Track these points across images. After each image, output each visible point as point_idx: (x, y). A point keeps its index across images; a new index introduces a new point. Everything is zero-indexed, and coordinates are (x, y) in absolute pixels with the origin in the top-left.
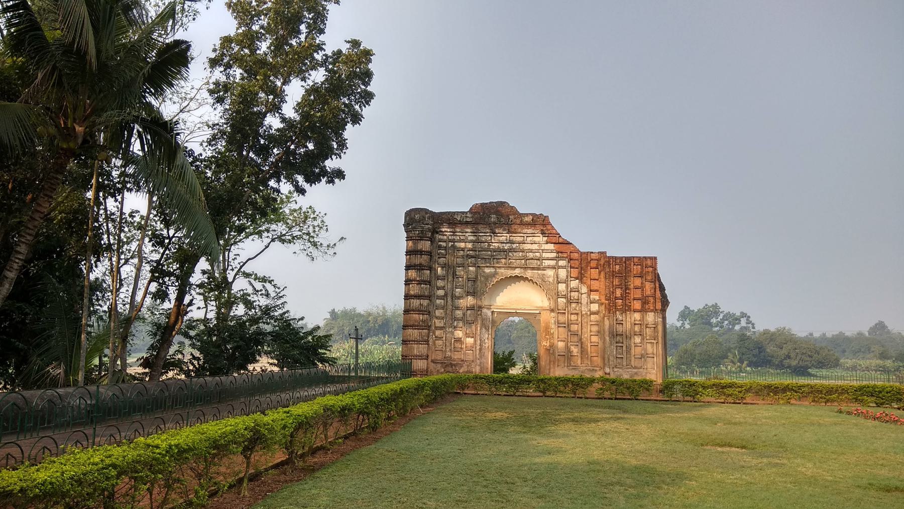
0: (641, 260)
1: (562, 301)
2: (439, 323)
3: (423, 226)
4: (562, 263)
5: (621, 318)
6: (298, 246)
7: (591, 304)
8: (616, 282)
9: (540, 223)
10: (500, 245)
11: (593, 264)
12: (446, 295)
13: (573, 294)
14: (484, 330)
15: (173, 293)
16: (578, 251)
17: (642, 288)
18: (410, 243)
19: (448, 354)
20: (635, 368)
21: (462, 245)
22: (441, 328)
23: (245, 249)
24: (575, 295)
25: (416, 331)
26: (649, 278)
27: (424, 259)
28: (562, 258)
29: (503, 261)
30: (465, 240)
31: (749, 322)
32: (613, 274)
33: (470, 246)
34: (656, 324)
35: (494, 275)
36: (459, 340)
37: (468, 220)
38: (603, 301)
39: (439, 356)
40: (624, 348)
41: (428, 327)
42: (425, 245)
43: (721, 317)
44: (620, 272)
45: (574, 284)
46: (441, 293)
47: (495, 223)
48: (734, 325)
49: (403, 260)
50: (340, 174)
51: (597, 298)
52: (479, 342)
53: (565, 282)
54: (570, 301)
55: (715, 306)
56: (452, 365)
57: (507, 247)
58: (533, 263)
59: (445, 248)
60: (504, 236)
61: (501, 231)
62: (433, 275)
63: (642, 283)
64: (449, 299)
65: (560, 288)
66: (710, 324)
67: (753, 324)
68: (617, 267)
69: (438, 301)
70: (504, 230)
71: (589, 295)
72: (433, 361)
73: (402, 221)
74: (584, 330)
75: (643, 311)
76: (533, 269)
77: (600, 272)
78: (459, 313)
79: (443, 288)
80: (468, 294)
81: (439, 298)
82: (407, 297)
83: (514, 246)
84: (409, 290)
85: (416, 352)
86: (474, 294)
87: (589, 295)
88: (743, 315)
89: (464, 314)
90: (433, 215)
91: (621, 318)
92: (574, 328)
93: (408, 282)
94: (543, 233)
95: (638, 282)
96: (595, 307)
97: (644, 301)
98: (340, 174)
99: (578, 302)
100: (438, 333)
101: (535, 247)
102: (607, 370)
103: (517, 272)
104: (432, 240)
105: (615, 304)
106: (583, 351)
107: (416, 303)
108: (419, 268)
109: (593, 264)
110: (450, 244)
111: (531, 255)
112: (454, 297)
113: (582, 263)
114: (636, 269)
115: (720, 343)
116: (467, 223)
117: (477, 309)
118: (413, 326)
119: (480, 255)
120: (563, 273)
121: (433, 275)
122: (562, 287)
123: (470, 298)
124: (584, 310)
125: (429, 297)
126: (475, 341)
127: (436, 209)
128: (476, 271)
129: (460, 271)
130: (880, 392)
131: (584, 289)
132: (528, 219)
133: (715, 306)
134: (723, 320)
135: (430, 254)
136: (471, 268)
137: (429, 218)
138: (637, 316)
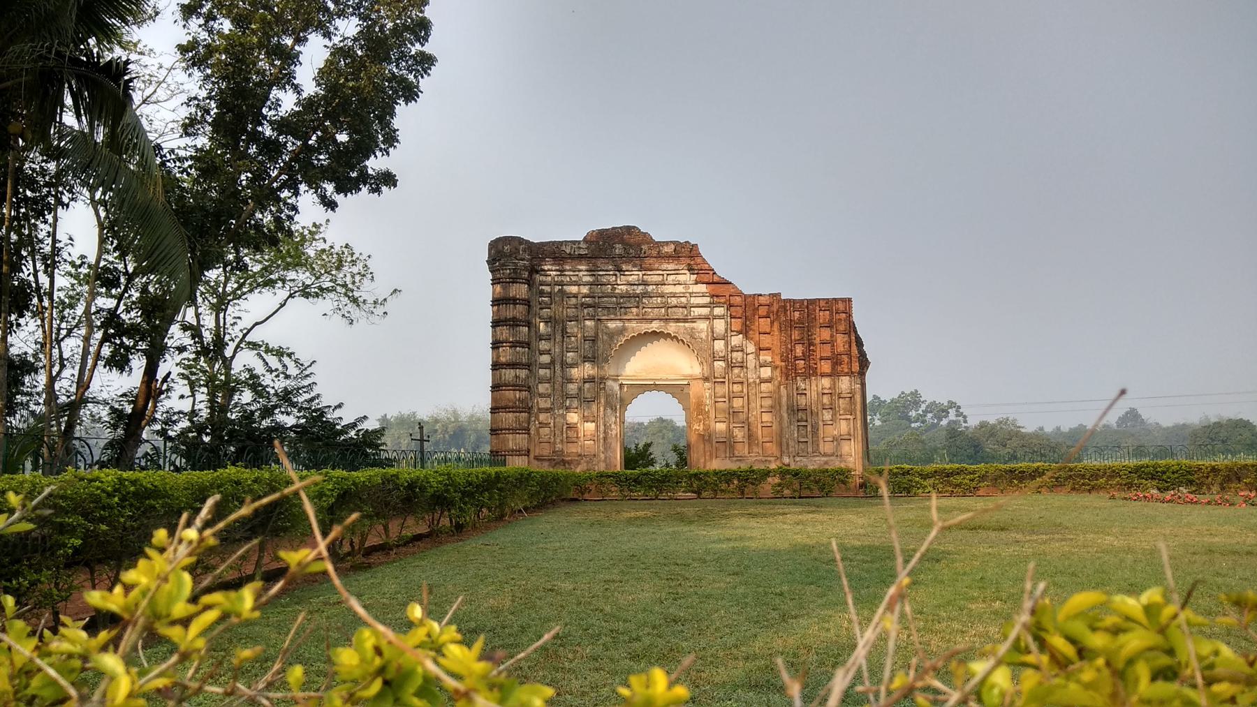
0: (830, 304)
1: (719, 365)
2: (544, 403)
3: (514, 262)
4: (718, 311)
5: (803, 386)
7: (761, 369)
8: (796, 335)
9: (686, 254)
10: (629, 288)
11: (763, 311)
12: (553, 362)
13: (735, 354)
14: (609, 410)
15: (138, 364)
16: (740, 294)
17: (832, 342)
18: (498, 288)
19: (559, 446)
20: (825, 455)
21: (574, 289)
22: (547, 410)
23: (253, 307)
24: (738, 356)
25: (511, 415)
26: (842, 328)
27: (518, 311)
28: (719, 305)
29: (634, 310)
31: (959, 414)
32: (791, 325)
33: (585, 290)
34: (852, 392)
35: (622, 331)
36: (571, 427)
37: (582, 252)
38: (778, 363)
39: (546, 451)
40: (809, 428)
41: (528, 410)
42: (520, 290)
43: (923, 407)
44: (800, 321)
45: (737, 340)
46: (545, 359)
47: (621, 257)
48: (940, 419)
49: (488, 313)
50: (388, 179)
51: (769, 359)
52: (602, 428)
54: (730, 366)
55: (915, 394)
56: (564, 462)
57: (639, 290)
59: (550, 295)
60: (635, 275)
61: (630, 268)
62: (533, 333)
63: (832, 336)
64: (558, 367)
65: (716, 347)
66: (909, 419)
67: (965, 417)
68: (797, 314)
69: (542, 372)
70: (635, 266)
71: (758, 356)
72: (536, 458)
73: (485, 256)
74: (752, 405)
75: (834, 374)
76: (678, 320)
77: (772, 323)
78: (572, 388)
79: (548, 352)
80: (586, 359)
81: (544, 366)
82: (496, 366)
83: (650, 288)
84: (498, 357)
85: (511, 445)
86: (592, 359)
87: (758, 356)
88: (952, 404)
89: (580, 389)
90: (530, 246)
91: (803, 386)
92: (737, 403)
93: (496, 345)
94: (690, 269)
95: (826, 334)
96: (766, 372)
97: (836, 361)
98: (388, 179)
99: (742, 366)
100: (542, 417)
101: (680, 289)
102: (786, 460)
103: (655, 326)
104: (530, 282)
105: (794, 368)
106: (751, 436)
107: (509, 374)
108: (513, 323)
109: (763, 311)
110: (557, 288)
111: (674, 301)
112: (565, 365)
113: (747, 311)
114: (823, 316)
115: (923, 442)
116: (581, 257)
117: (598, 382)
118: (506, 408)
119: (600, 304)
120: (720, 326)
121: (533, 333)
122: (719, 345)
123: (587, 365)
124: (752, 376)
125: (528, 366)
126: (597, 427)
127: (535, 237)
128: (597, 328)
129: (572, 327)
130: (1164, 473)
131: (751, 348)
132: (669, 249)
133: (915, 394)
134: (925, 412)
135: (527, 302)
136: (588, 323)
137: (524, 251)
138: (826, 382)
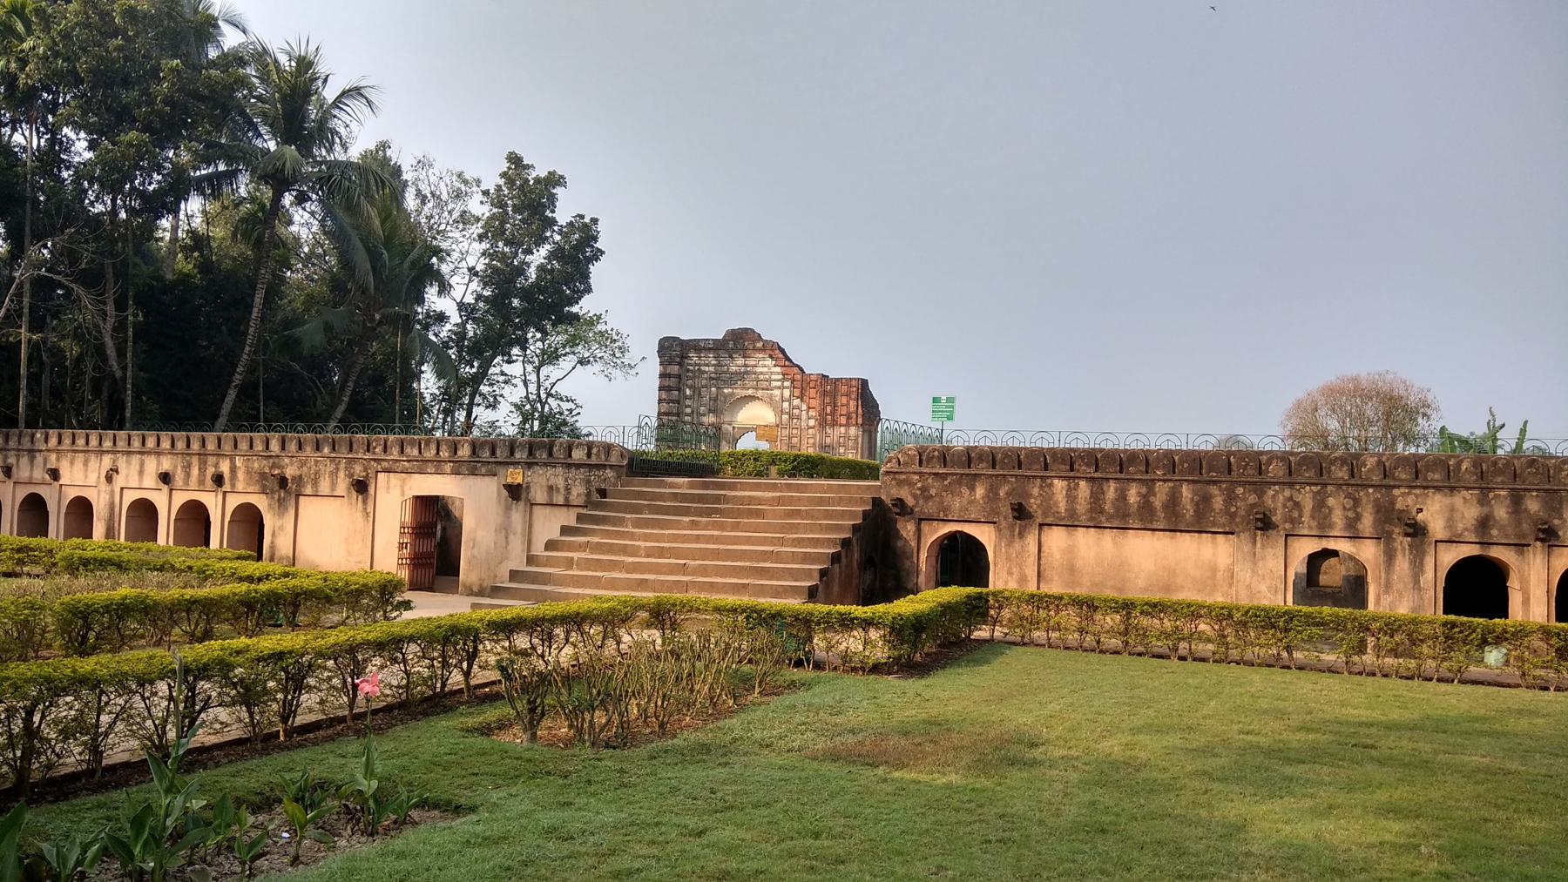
3: (674, 352)
4: (787, 384)
6: (597, 367)
8: (827, 400)
17: (847, 405)
24: (796, 412)
27: (673, 382)
30: (708, 364)
35: (732, 394)
42: (675, 369)
45: (796, 402)
46: (688, 410)
49: (657, 382)
53: (789, 401)
54: (791, 417)
58: (762, 384)
60: (740, 361)
75: (847, 425)
92: (795, 440)
93: (660, 401)
95: (844, 400)
96: (812, 422)
97: (849, 418)
99: (799, 418)
103: (750, 392)
104: (680, 364)
107: (665, 419)
120: (787, 393)
122: (786, 405)
124: (804, 425)
125: (678, 415)
131: (804, 407)
135: (679, 377)
138: (843, 429)
